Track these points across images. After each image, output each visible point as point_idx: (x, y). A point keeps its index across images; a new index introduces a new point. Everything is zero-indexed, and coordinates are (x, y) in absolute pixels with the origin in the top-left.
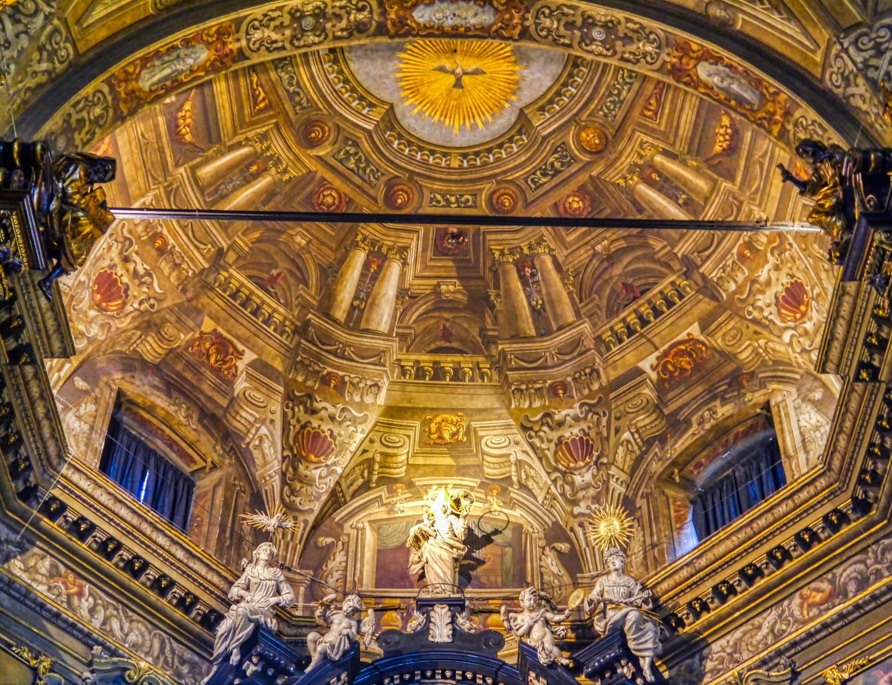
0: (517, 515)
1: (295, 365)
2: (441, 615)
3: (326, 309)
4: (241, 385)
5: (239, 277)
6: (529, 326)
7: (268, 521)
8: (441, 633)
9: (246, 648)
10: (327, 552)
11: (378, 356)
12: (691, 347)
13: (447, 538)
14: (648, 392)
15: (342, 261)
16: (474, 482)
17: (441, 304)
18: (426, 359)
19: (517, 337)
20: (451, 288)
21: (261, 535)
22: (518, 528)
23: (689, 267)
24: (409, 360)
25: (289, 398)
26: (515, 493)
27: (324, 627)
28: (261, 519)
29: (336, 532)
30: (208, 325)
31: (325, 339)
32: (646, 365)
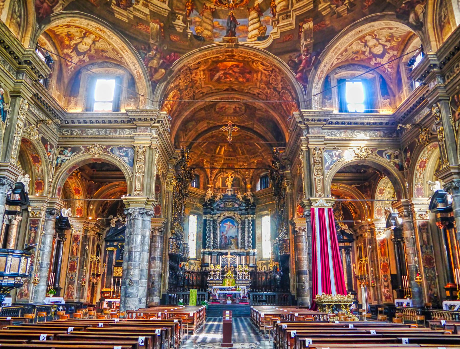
0: (239, 176)
1: (211, 159)
2: (229, 192)
3: (215, 153)
4: (205, 163)
5: (204, 153)
6: (241, 154)
7: (210, 186)
8: (230, 194)
9: (209, 201)
10: (216, 182)
11: (221, 157)
12: (260, 161)
13: (230, 181)
14: (255, 164)
15: (217, 147)
16: (233, 171)
17: (229, 151)
18: (228, 158)
19: (239, 155)
20: (231, 150)
21: (208, 188)
22: (239, 178)
23: (261, 153)
24: (225, 158)
25: (211, 164)
26: (239, 173)
27: (216, 197)
28: (209, 186)
29: (217, 179)
30: (201, 158)
31: (214, 156)
32: (255, 161)
